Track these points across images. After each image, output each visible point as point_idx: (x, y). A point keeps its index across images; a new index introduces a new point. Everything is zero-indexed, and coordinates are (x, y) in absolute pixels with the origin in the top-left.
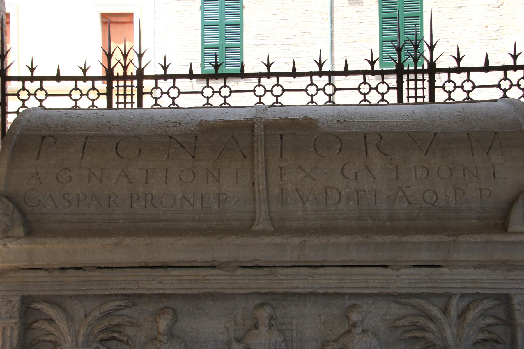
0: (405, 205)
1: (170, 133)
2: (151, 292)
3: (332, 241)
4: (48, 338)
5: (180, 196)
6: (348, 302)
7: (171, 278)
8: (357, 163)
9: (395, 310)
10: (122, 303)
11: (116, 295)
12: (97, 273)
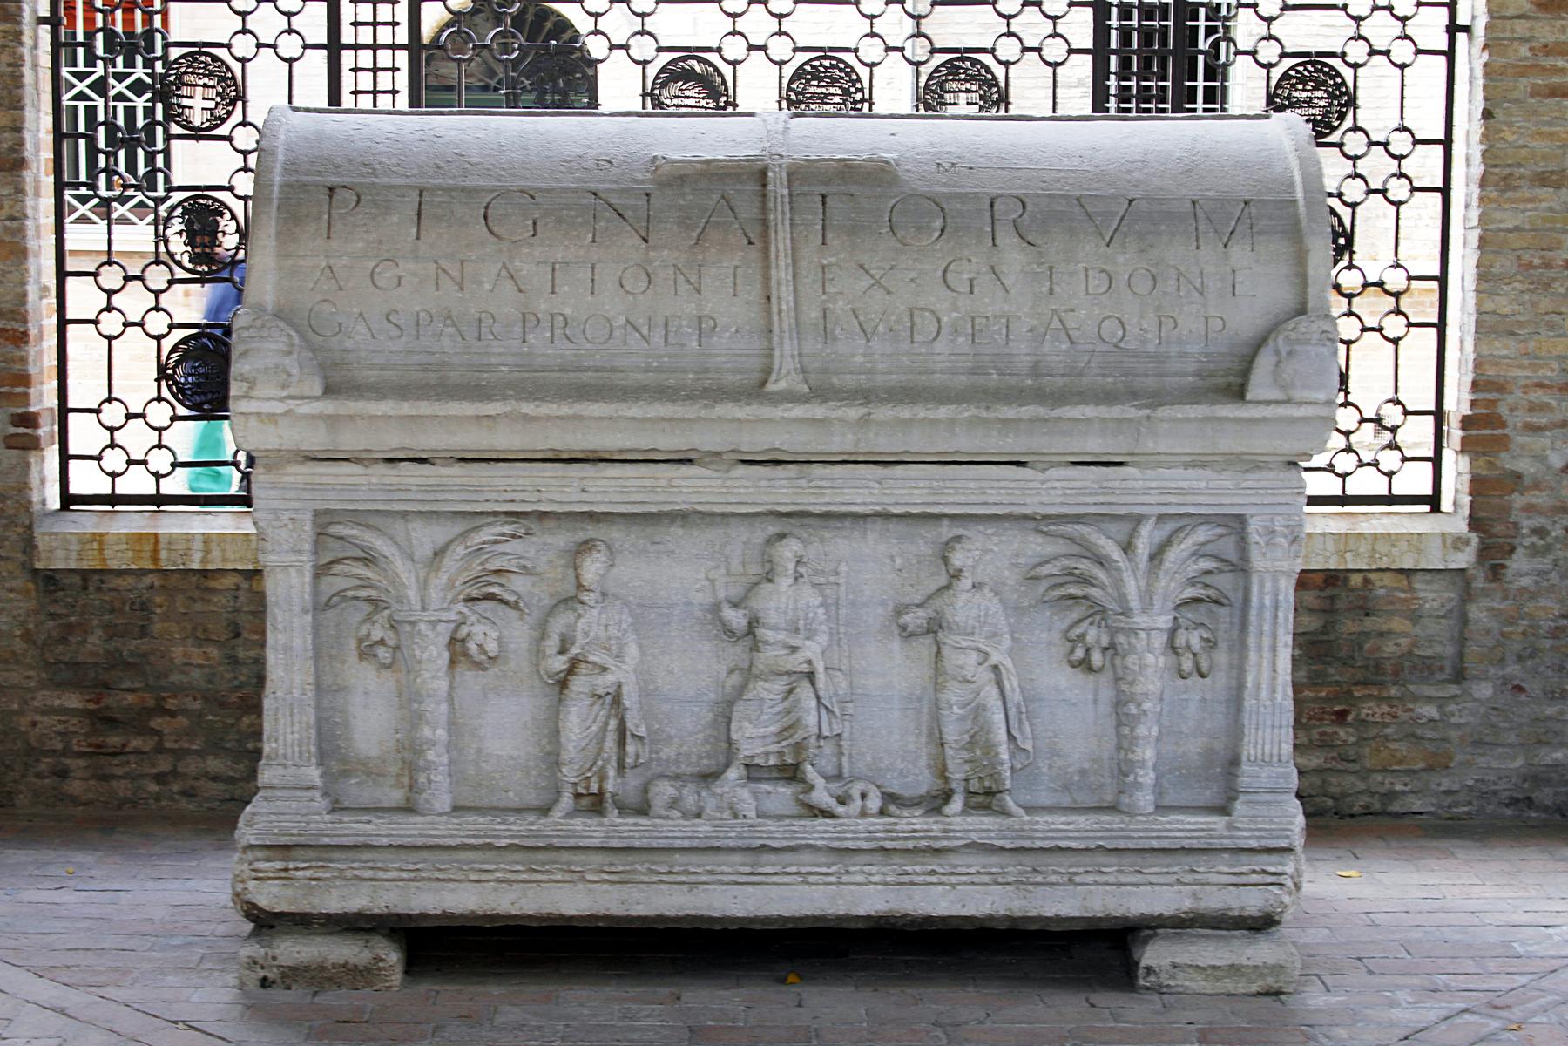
0: (1064, 347)
1: (593, 186)
2: (567, 508)
3: (922, 415)
4: (363, 593)
5: (622, 320)
6: (946, 531)
7: (604, 482)
8: (974, 260)
9: (1035, 546)
10: (507, 529)
11: (495, 514)
12: (457, 469)
